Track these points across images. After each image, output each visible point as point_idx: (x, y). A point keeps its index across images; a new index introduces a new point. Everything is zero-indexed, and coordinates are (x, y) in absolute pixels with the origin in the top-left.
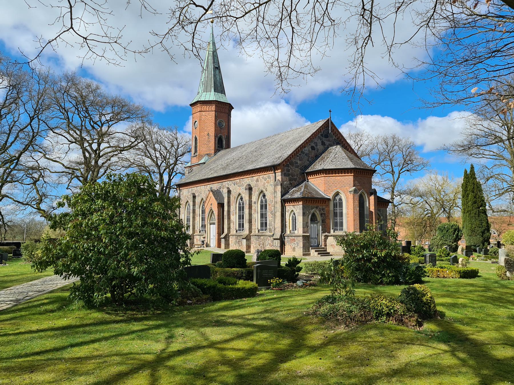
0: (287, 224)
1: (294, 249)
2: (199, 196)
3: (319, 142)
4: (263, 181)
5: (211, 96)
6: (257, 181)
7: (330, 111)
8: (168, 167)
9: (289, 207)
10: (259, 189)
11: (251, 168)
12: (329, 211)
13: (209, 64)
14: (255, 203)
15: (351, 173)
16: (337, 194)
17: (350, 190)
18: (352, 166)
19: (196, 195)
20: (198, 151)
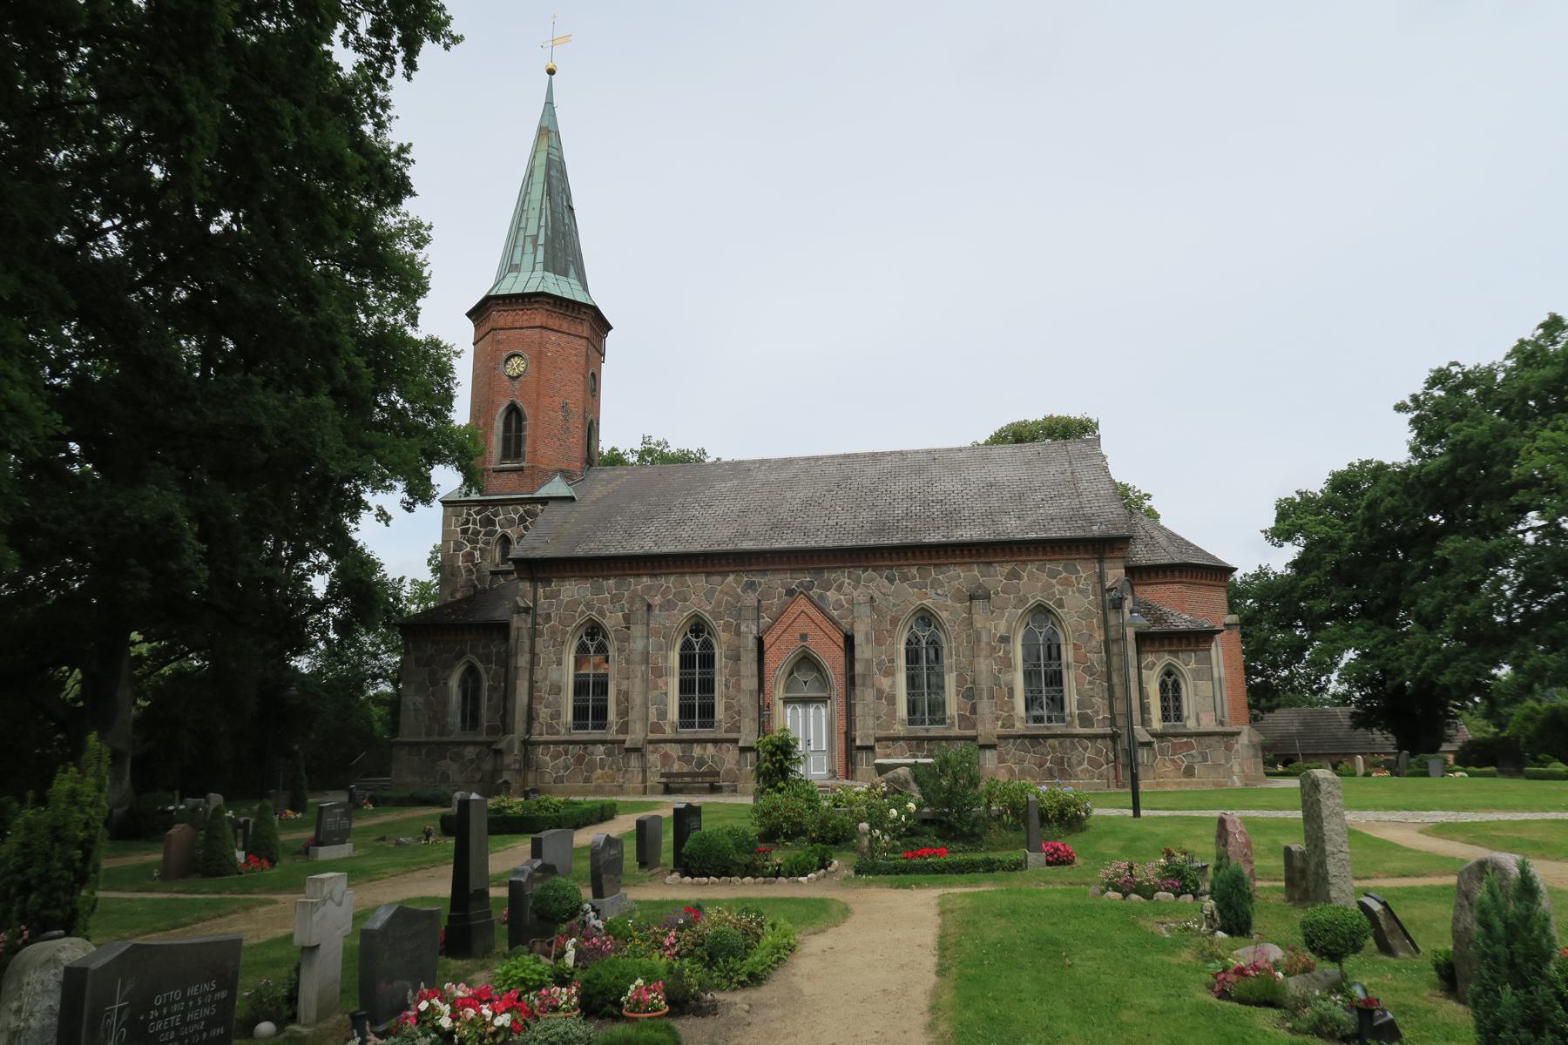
1: (1189, 772)
2: (668, 606)
4: (1044, 577)
6: (1014, 575)
10: (1022, 601)
13: (554, 191)
14: (1005, 639)
19: (657, 600)
20: (528, 456)
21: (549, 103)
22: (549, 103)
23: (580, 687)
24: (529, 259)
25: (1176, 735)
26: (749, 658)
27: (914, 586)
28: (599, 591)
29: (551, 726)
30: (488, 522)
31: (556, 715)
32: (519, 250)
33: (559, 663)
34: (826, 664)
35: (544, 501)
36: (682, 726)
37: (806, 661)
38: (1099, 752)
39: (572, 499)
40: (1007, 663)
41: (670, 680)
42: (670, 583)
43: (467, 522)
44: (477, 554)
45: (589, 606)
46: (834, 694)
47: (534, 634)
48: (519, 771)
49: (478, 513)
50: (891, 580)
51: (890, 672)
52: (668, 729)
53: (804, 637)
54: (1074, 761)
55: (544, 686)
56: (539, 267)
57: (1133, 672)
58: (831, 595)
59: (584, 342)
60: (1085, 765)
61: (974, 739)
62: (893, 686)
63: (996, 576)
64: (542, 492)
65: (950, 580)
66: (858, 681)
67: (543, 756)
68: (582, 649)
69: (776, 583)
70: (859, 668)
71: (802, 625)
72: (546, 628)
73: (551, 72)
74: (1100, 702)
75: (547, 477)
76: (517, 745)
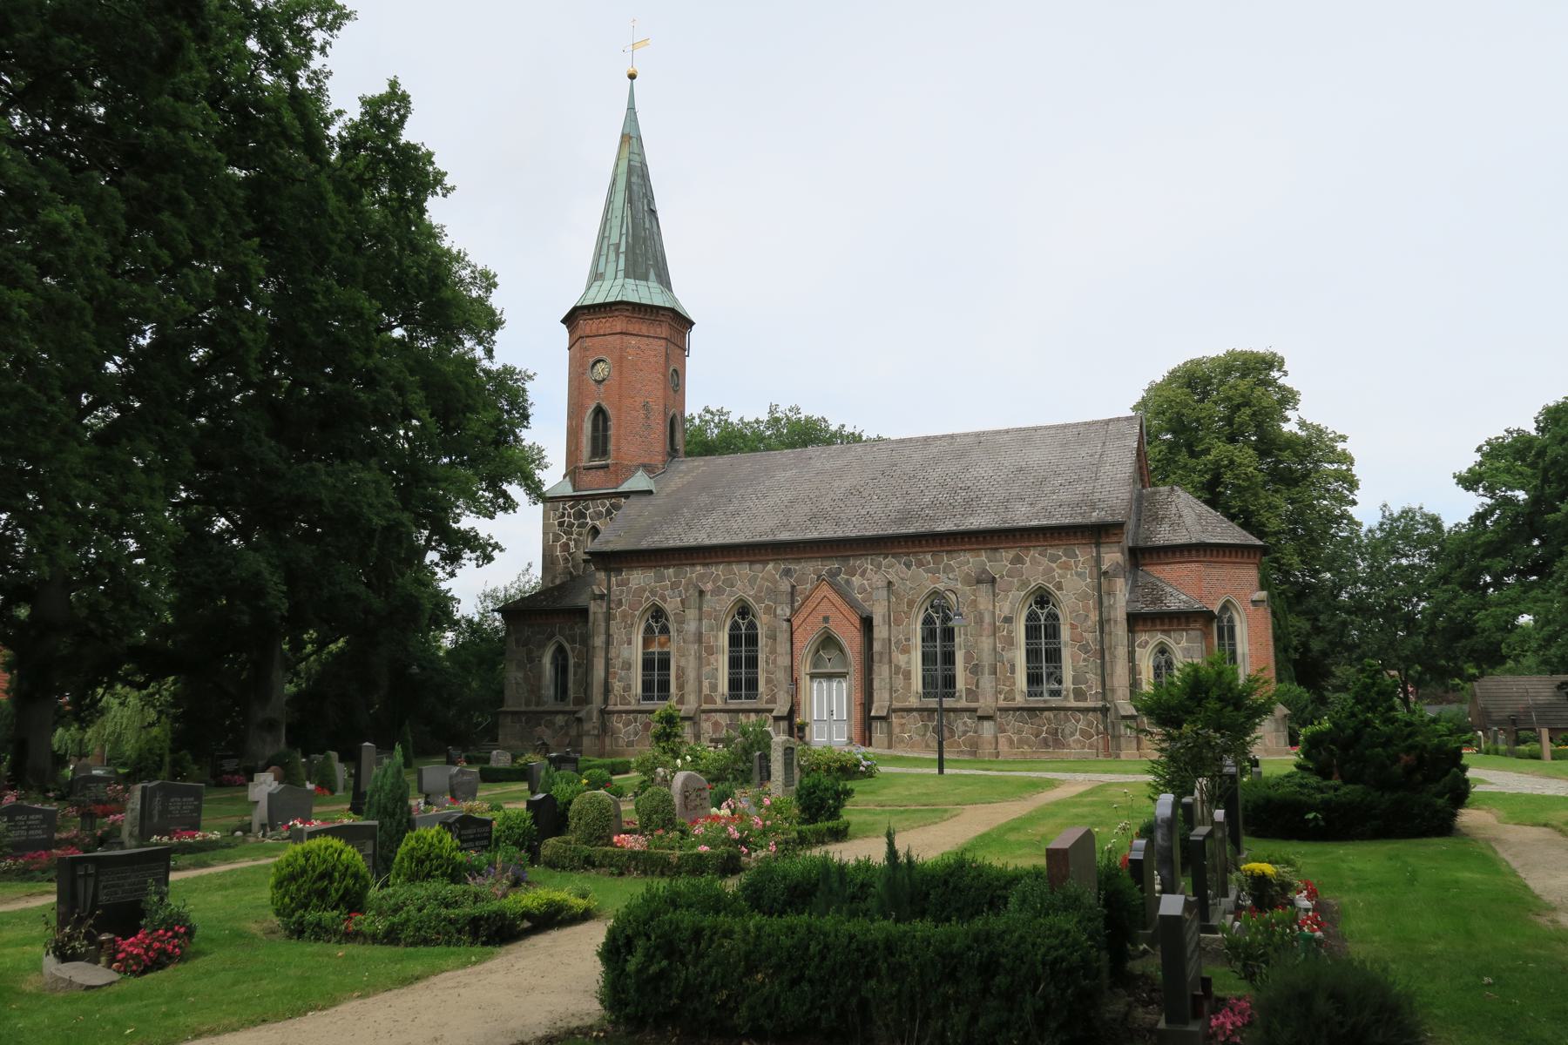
2: (718, 591)
5: (645, 293)
6: (1018, 560)
10: (1024, 584)
13: (635, 198)
14: (1008, 620)
16: (1225, 607)
19: (709, 586)
21: (631, 109)
22: (631, 109)
23: (648, 664)
24: (611, 266)
26: (783, 637)
27: (927, 571)
28: (661, 578)
29: (623, 698)
30: (581, 515)
31: (627, 688)
32: (603, 259)
33: (630, 643)
34: (844, 643)
35: (627, 495)
36: (732, 697)
37: (828, 641)
38: (1090, 724)
39: (650, 492)
40: (1010, 642)
41: (720, 657)
42: (719, 570)
43: (563, 515)
44: (572, 544)
45: (653, 593)
46: (852, 669)
47: (609, 617)
48: (598, 736)
49: (572, 507)
50: (908, 566)
51: (906, 650)
52: (718, 700)
53: (826, 619)
54: (1067, 732)
55: (618, 663)
56: (621, 274)
57: (1122, 652)
58: (856, 580)
60: (1078, 736)
61: (975, 710)
62: (908, 662)
63: (1000, 562)
64: (625, 487)
65: (961, 564)
66: (876, 658)
67: (617, 724)
68: (649, 630)
69: (809, 569)
70: (877, 647)
71: (825, 608)
72: (618, 612)
73: (632, 77)
74: (1093, 678)
75: (630, 472)
76: (595, 714)
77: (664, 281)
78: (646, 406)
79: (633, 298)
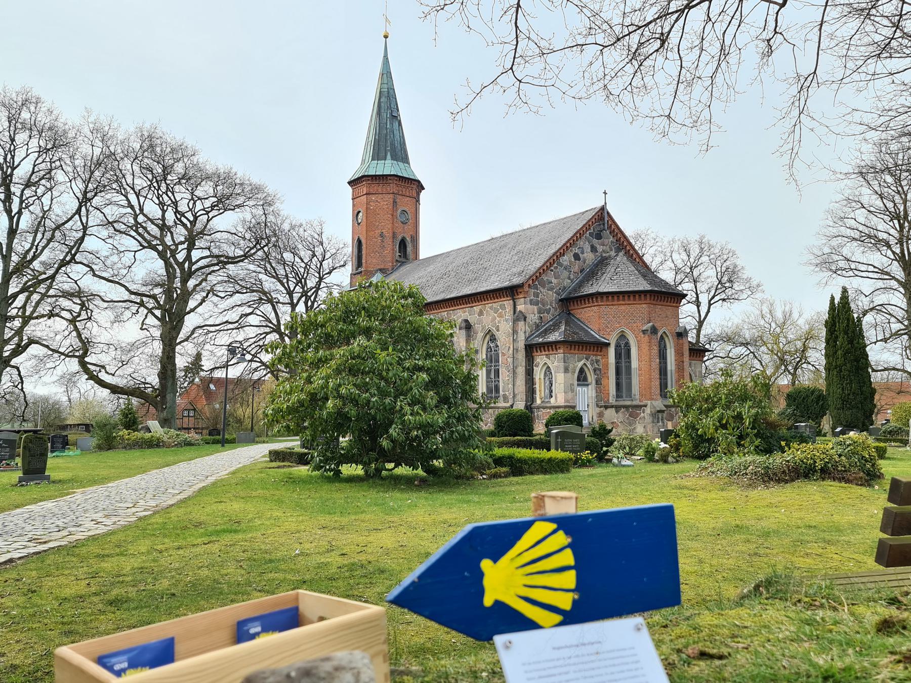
0: (537, 386)
3: (587, 248)
4: (492, 312)
5: (387, 167)
6: (481, 313)
7: (605, 193)
8: (304, 294)
9: (541, 359)
11: (469, 292)
12: (606, 366)
15: (645, 299)
17: (644, 328)
18: (648, 287)
20: (364, 265)
25: (547, 408)
57: (521, 371)
59: (391, 196)
73: (386, 37)
77: (405, 159)
78: (382, 235)
79: (372, 172)
